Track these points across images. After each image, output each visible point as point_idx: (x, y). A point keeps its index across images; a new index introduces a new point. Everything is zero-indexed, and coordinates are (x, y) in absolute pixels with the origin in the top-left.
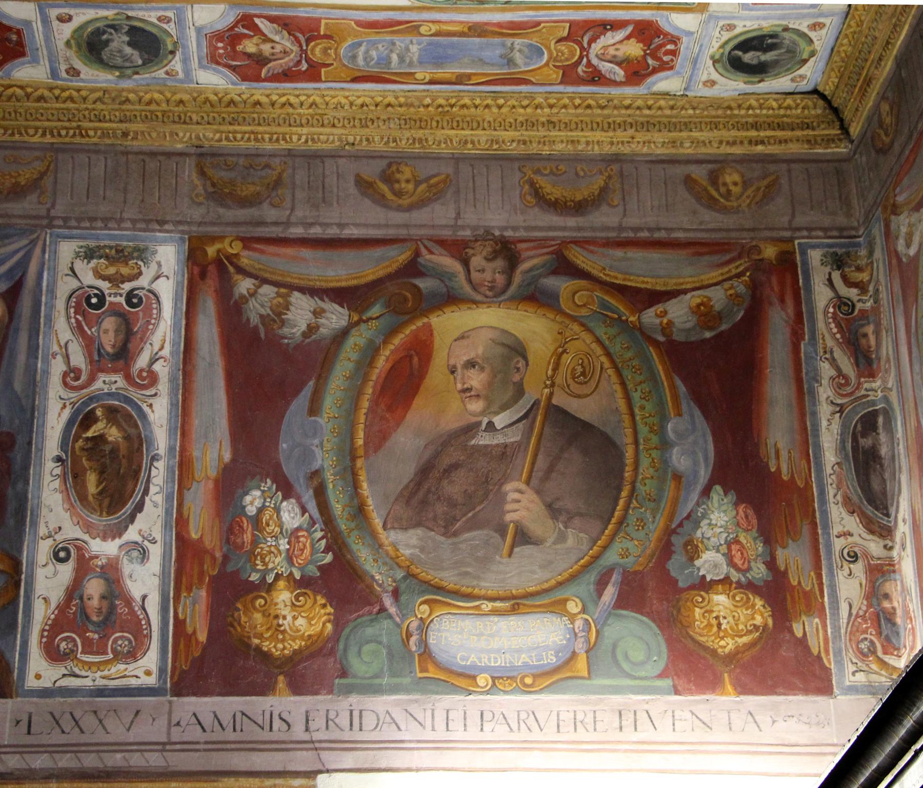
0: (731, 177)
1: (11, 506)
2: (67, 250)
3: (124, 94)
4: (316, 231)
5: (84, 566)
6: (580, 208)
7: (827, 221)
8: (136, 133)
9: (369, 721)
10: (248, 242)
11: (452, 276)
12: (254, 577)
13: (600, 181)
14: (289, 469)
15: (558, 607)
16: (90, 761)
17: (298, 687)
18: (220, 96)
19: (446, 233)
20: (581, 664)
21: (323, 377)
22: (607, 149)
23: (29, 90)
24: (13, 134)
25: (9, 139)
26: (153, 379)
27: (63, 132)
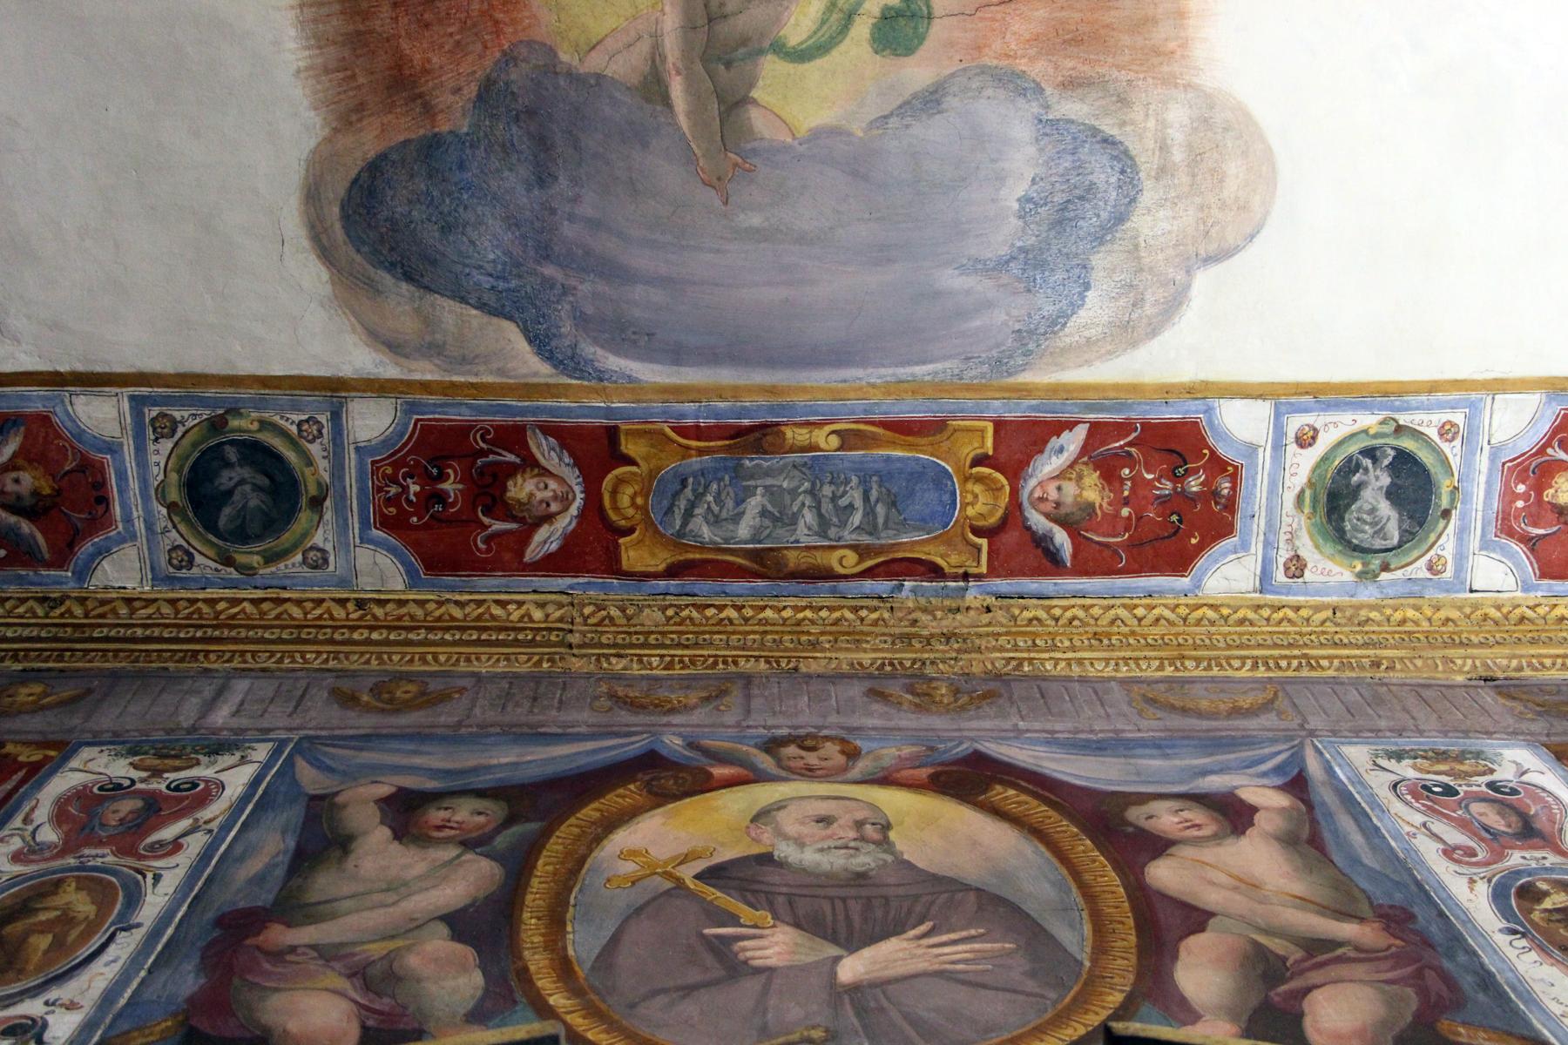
3: (1363, 613)
8: (1392, 660)
18: (1505, 610)
23: (1225, 611)
24: (1209, 668)
25: (1204, 674)
27: (1283, 663)
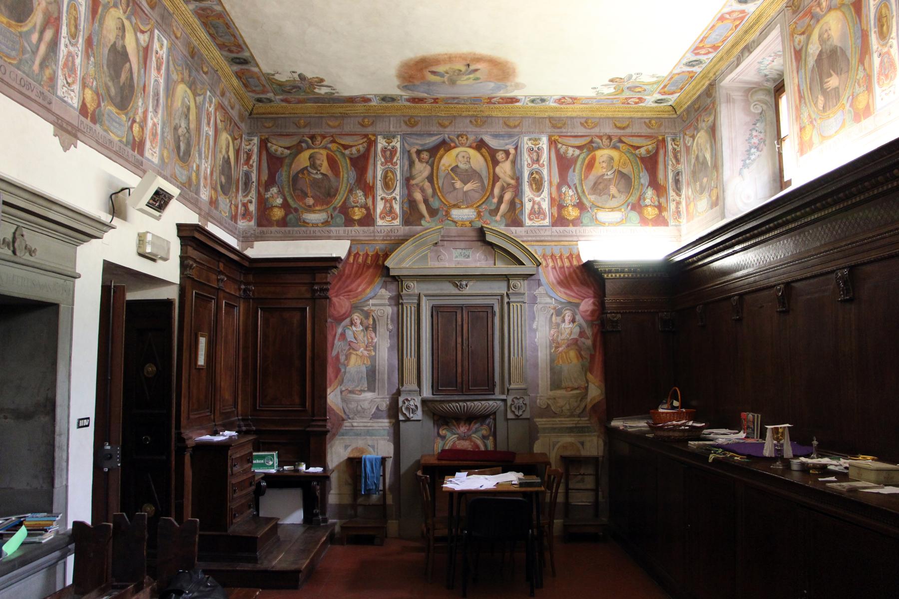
0: (653, 122)
1: (520, 191)
2: (526, 139)
4: (573, 134)
5: (534, 203)
6: (624, 128)
7: (671, 131)
9: (587, 232)
10: (560, 136)
11: (599, 143)
12: (565, 205)
13: (628, 123)
14: (570, 183)
15: (620, 210)
16: (538, 239)
17: (574, 225)
19: (598, 134)
20: (624, 221)
21: (575, 164)
22: (629, 116)
26: (544, 165)
